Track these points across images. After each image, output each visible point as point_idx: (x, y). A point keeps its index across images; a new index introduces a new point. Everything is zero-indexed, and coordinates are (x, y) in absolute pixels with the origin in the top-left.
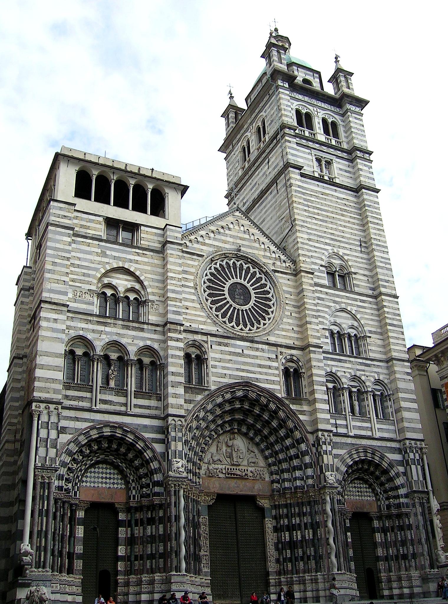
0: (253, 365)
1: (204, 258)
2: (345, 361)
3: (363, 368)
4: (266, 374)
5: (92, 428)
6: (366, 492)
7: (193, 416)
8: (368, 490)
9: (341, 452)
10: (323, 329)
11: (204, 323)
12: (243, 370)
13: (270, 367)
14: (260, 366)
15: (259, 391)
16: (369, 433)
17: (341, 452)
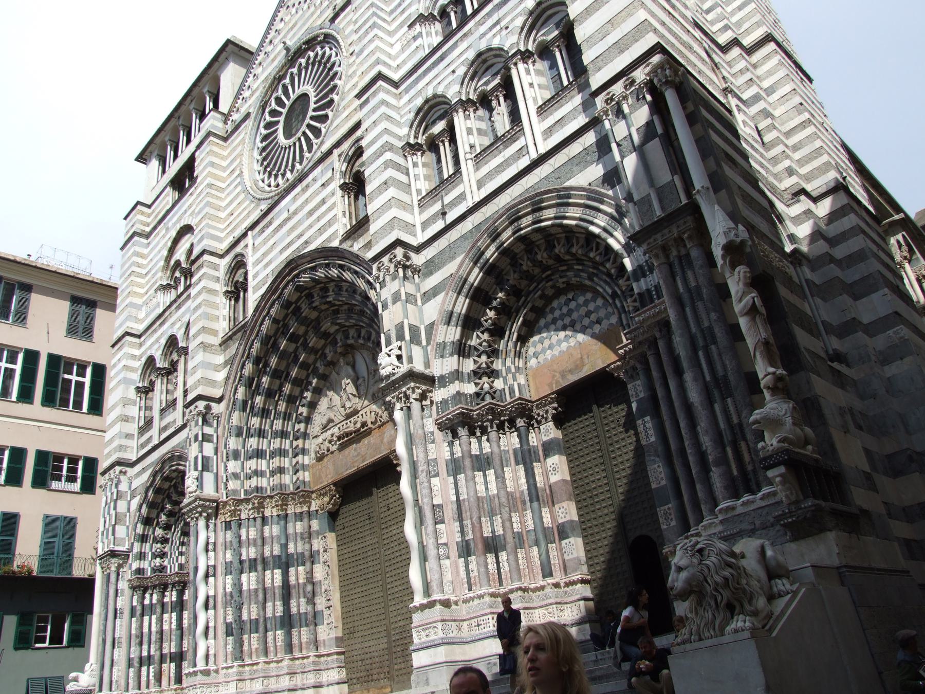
0: (300, 222)
1: (253, 116)
2: (455, 45)
3: (495, 18)
4: (319, 219)
5: (154, 475)
6: (588, 314)
7: (234, 382)
8: (591, 306)
9: (450, 268)
10: (410, 27)
11: (248, 215)
12: (289, 245)
13: (323, 201)
14: (311, 213)
15: (310, 262)
16: (524, 162)
17: (450, 268)
